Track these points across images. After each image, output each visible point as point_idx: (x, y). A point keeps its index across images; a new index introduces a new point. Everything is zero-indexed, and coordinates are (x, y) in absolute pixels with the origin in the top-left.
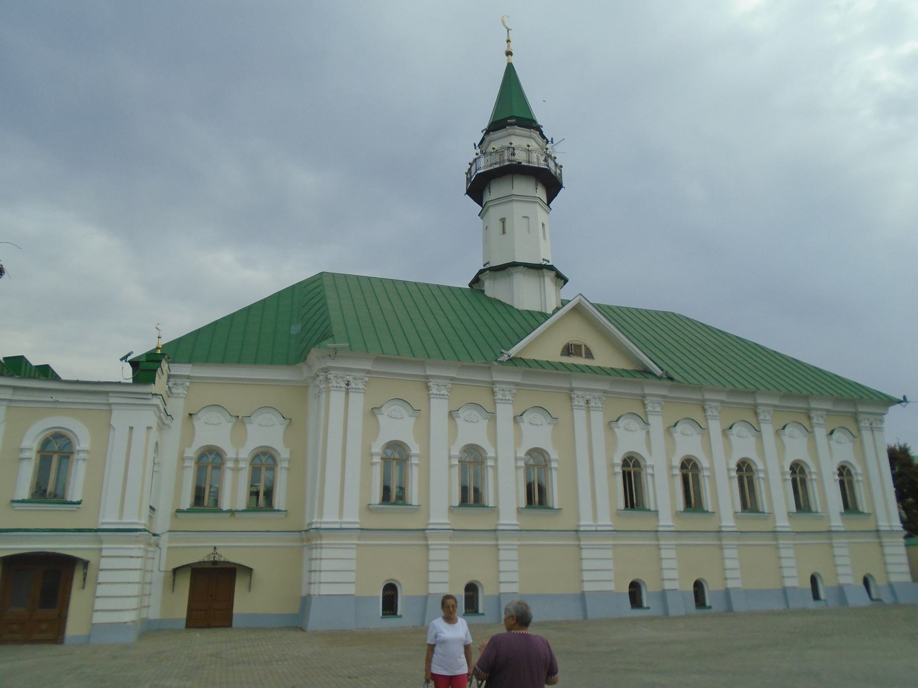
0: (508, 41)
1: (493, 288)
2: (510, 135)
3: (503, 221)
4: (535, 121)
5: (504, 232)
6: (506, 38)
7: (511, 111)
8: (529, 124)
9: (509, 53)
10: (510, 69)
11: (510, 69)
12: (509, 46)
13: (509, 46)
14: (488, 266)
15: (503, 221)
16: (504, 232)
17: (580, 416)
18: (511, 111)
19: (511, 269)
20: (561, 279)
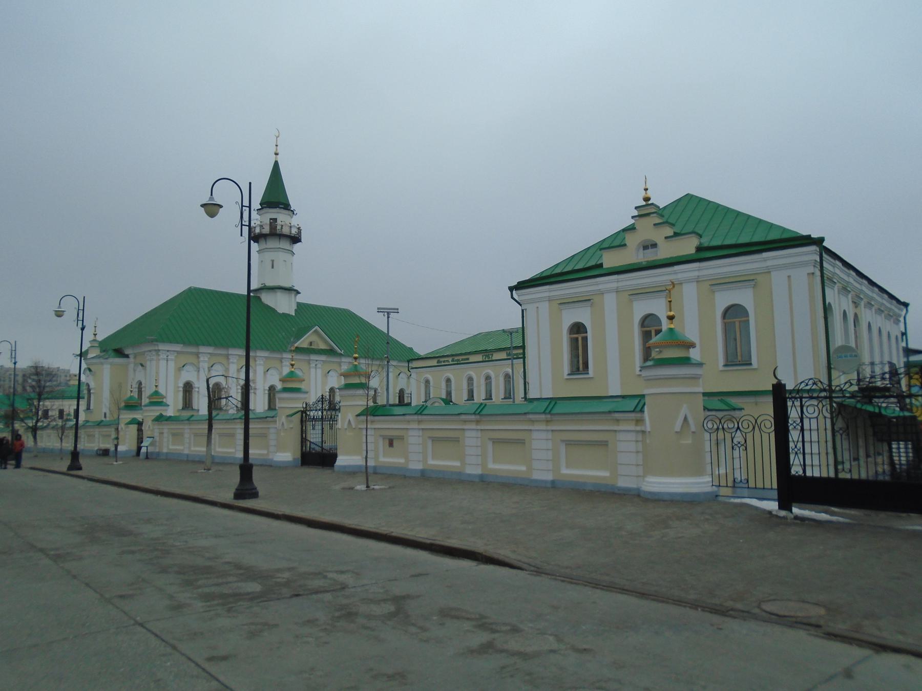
1: (267, 299)
3: (273, 261)
4: (289, 205)
8: (286, 207)
9: (276, 154)
10: (276, 164)
11: (276, 164)
15: (273, 261)
17: (313, 371)
20: (298, 293)
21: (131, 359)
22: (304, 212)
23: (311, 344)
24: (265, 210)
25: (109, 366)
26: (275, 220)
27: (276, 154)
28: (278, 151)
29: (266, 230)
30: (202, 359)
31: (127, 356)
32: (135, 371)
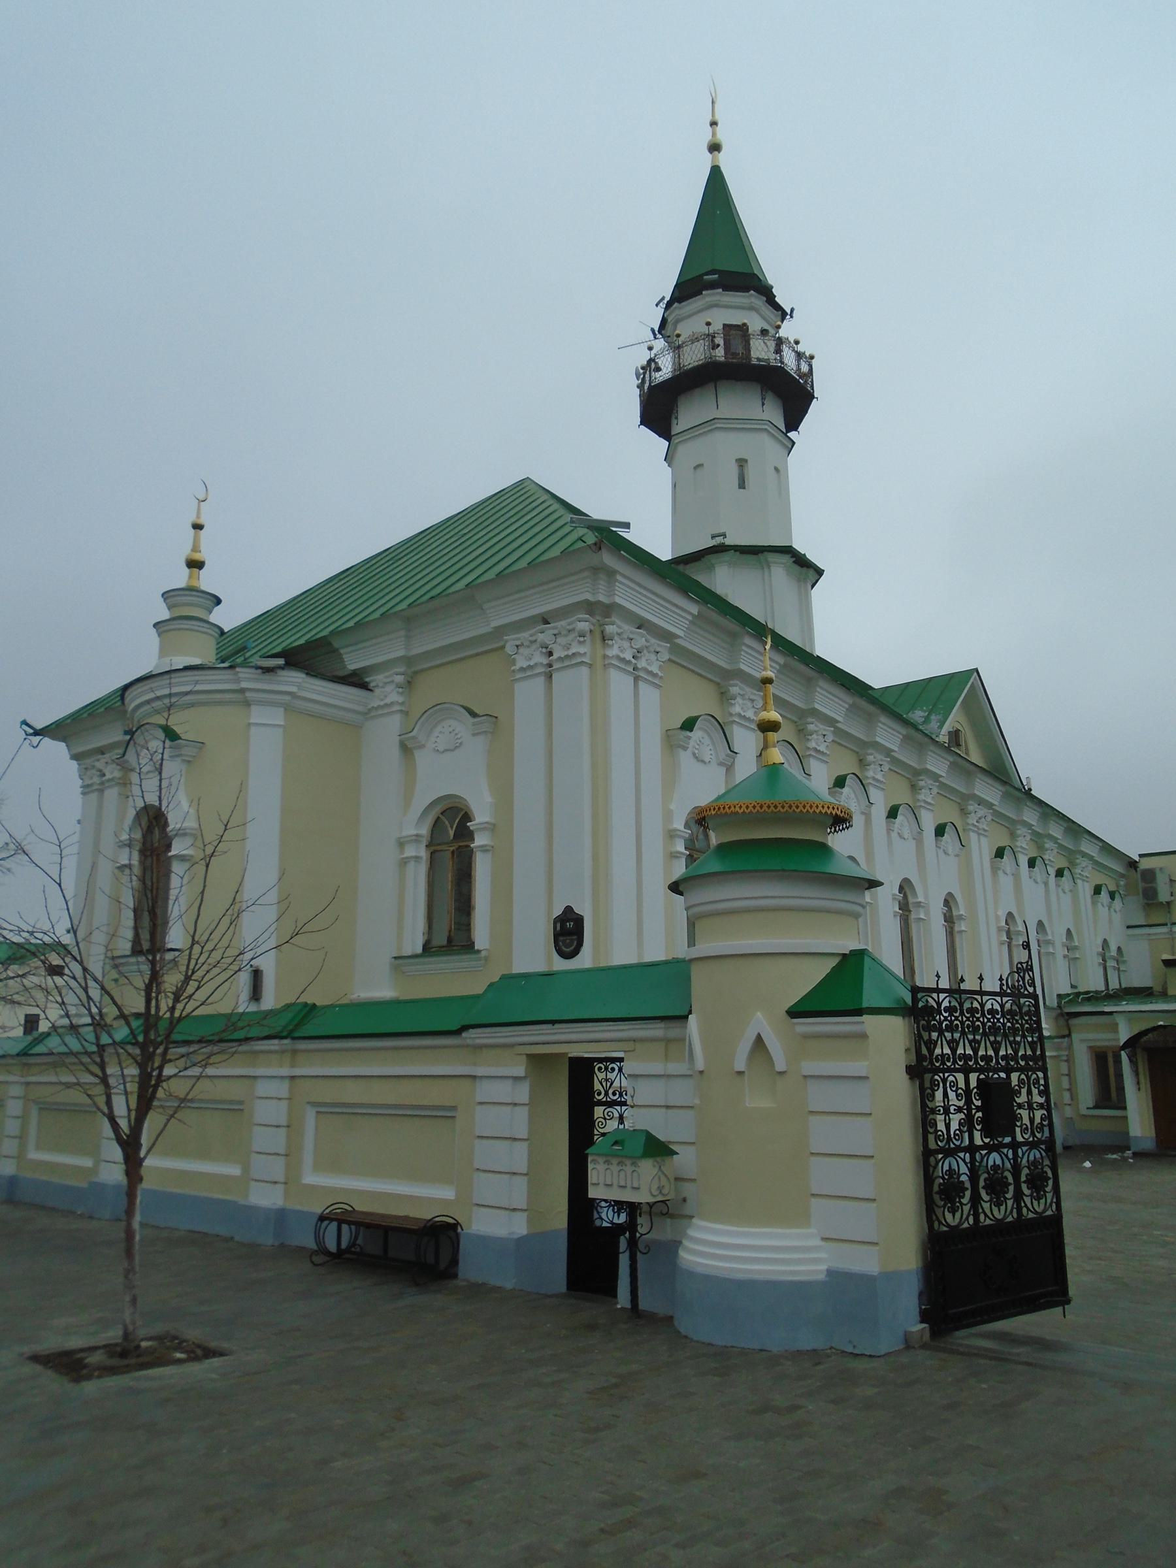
0: (714, 124)
2: (752, 308)
3: (742, 463)
5: (742, 485)
6: (709, 118)
7: (719, 261)
9: (714, 148)
10: (716, 180)
11: (716, 180)
12: (714, 134)
13: (714, 134)
14: (719, 540)
15: (742, 463)
16: (742, 485)
18: (719, 261)
19: (771, 557)
21: (387, 690)
22: (817, 324)
23: (955, 735)
24: (709, 297)
25: (277, 717)
26: (743, 329)
27: (714, 148)
28: (722, 135)
29: (720, 354)
30: (737, 709)
31: (357, 680)
32: (406, 749)
